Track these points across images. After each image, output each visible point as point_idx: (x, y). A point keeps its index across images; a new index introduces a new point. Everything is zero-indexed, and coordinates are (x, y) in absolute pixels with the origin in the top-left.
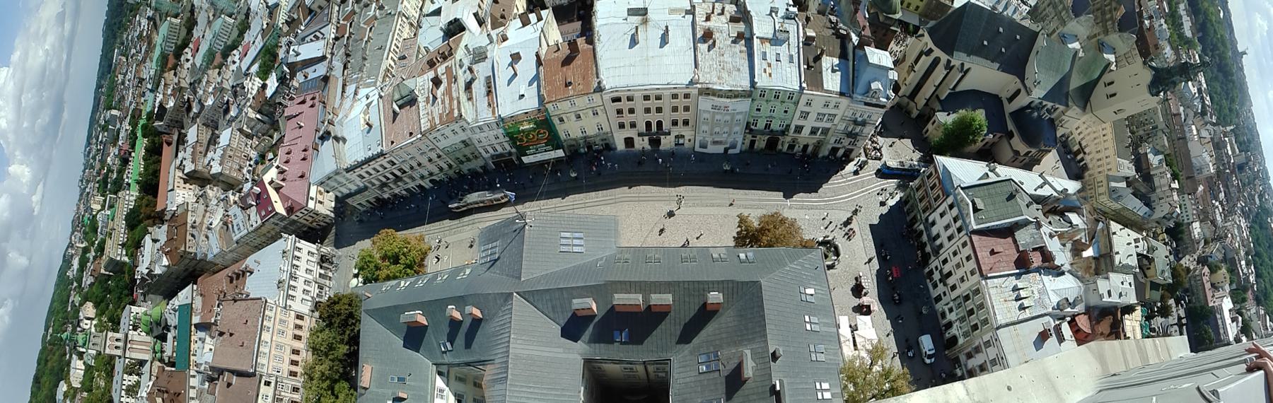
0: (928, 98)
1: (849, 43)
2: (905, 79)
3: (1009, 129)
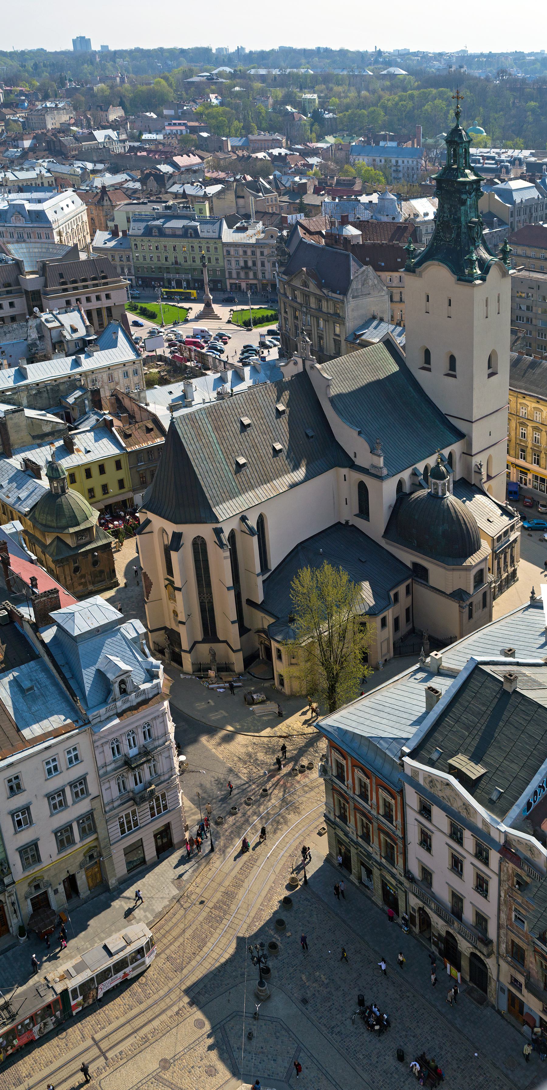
0: (235, 618)
1: (22, 627)
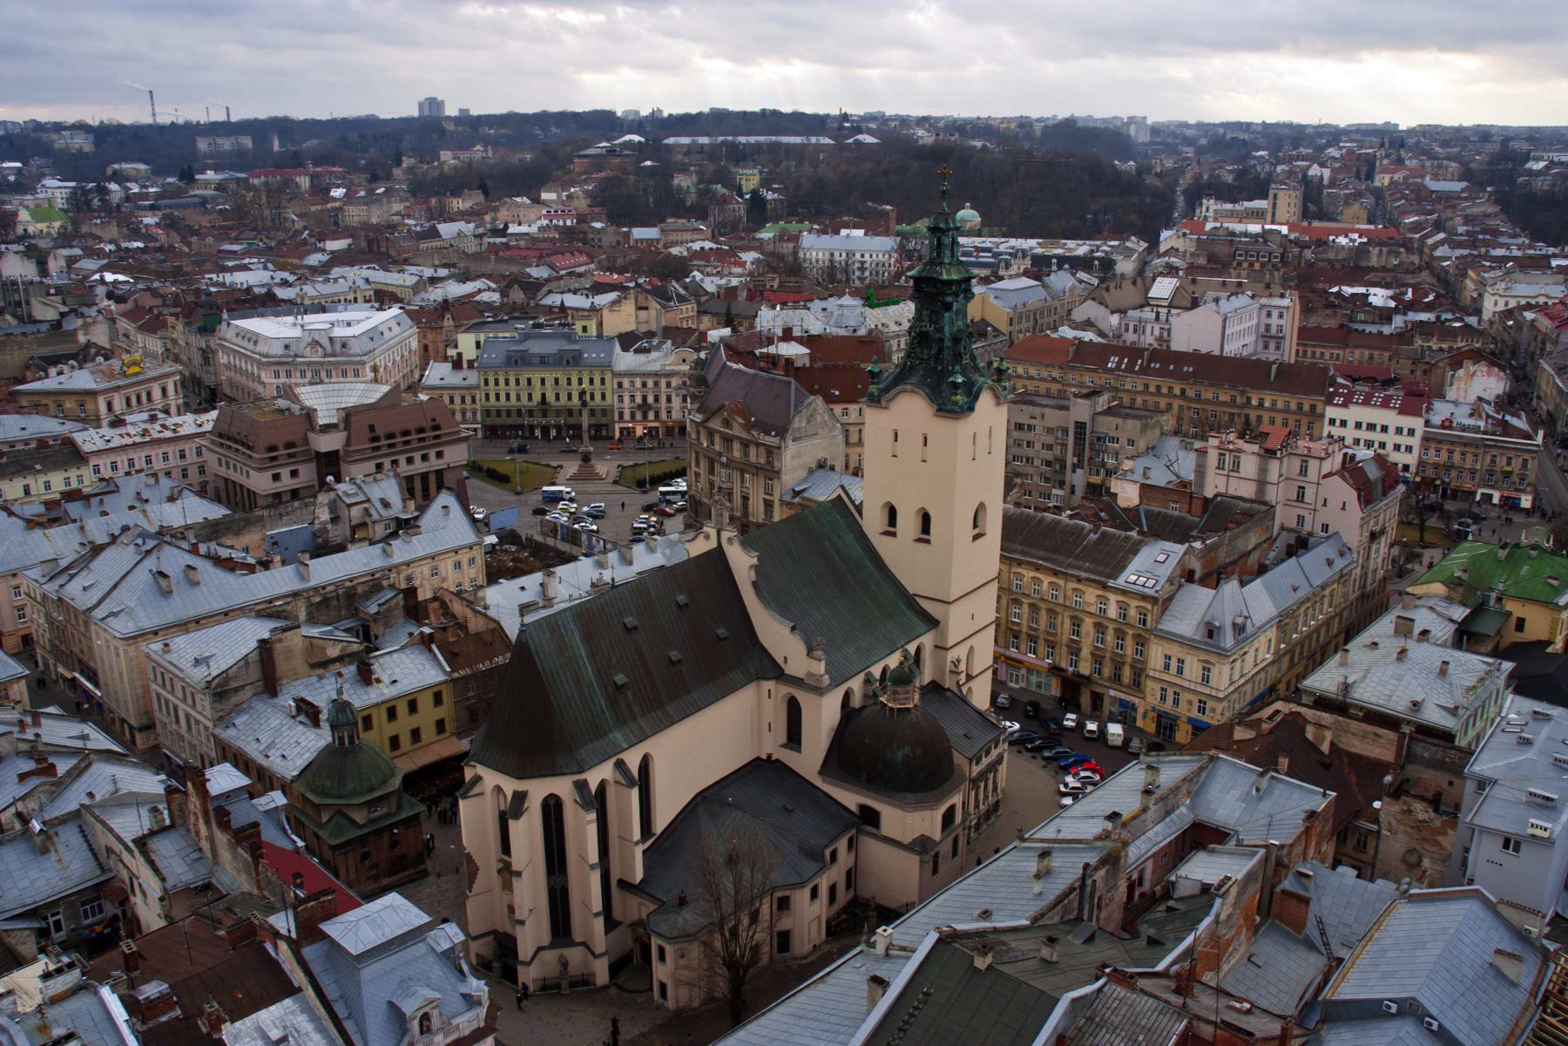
2: (511, 909)
3: (853, 808)
